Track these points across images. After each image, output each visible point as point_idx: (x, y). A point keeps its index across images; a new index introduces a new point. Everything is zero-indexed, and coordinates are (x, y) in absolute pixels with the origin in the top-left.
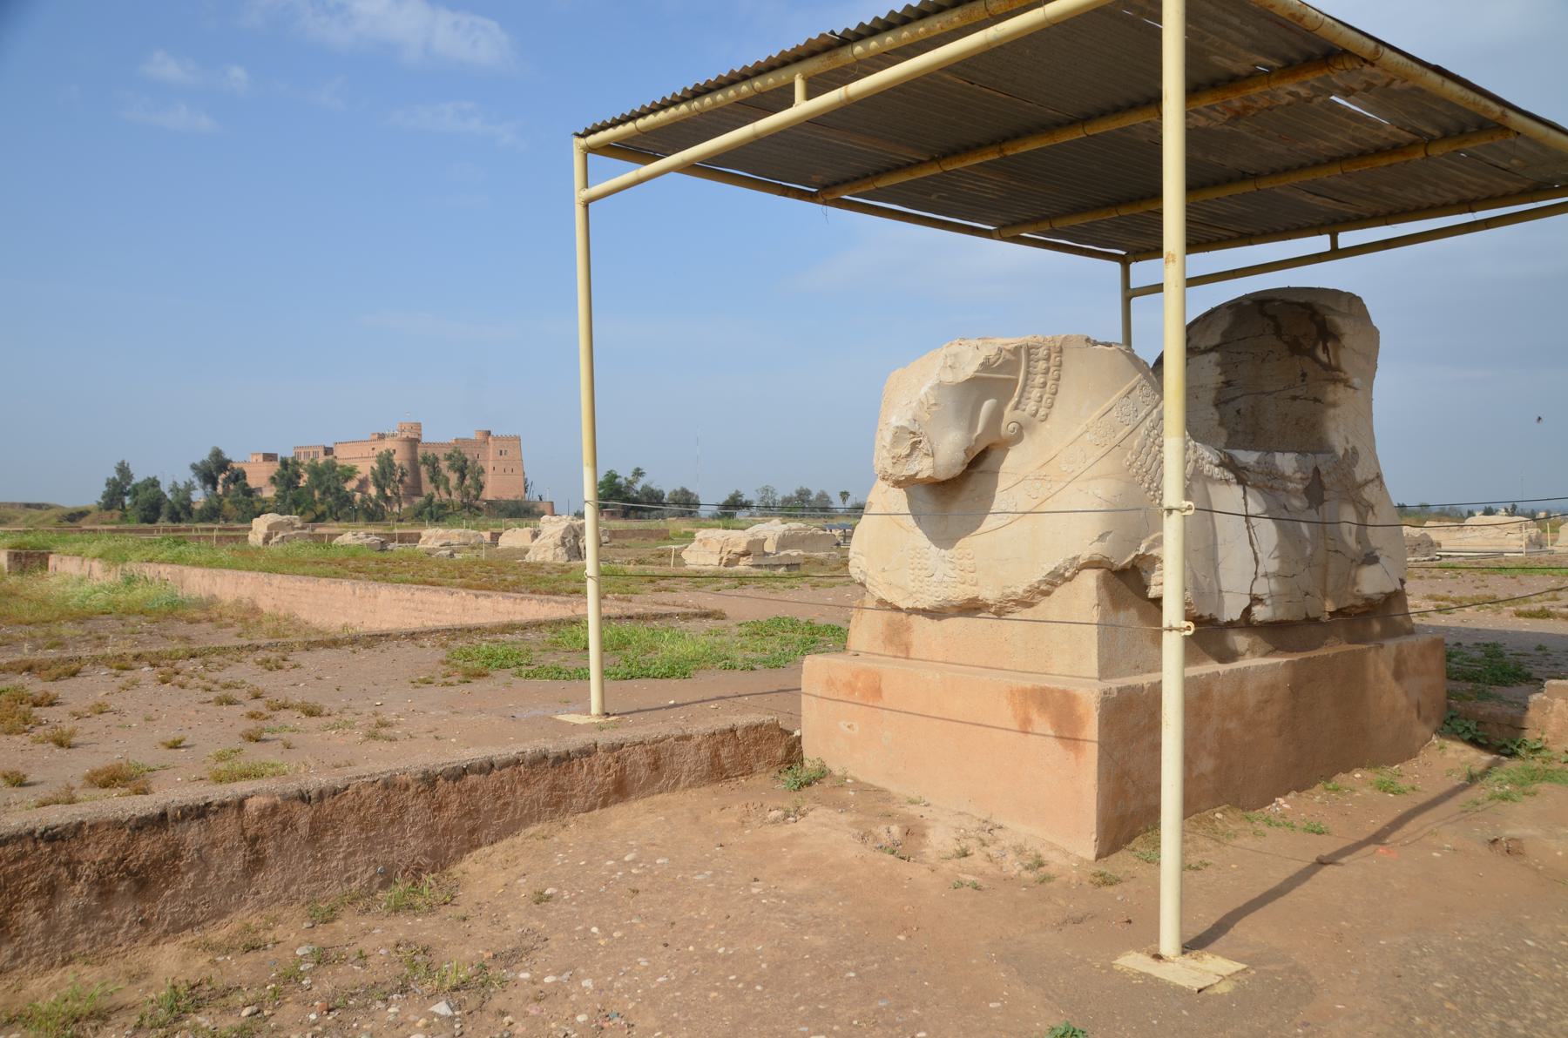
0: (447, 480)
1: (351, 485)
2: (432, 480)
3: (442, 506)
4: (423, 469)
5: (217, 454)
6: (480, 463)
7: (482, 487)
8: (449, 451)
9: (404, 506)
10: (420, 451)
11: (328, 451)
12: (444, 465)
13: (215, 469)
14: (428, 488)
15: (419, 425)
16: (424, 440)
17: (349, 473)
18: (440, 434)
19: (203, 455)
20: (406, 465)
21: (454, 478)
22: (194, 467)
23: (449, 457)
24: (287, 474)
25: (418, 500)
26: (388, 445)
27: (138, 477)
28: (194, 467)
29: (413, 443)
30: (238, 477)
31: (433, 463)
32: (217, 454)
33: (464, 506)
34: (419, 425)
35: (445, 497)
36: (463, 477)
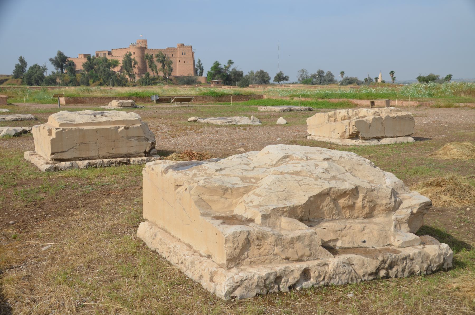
0: (156, 67)
1: (117, 69)
2: (150, 66)
3: (154, 79)
4: (147, 61)
5: (60, 54)
6: (172, 59)
7: (172, 70)
8: (157, 53)
9: (138, 78)
10: (146, 53)
11: (110, 53)
12: (155, 59)
13: (61, 61)
14: (149, 70)
15: (146, 41)
16: (148, 48)
17: (115, 64)
18: (155, 45)
19: (54, 55)
20: (138, 59)
21: (159, 66)
22: (51, 60)
23: (157, 56)
24: (91, 63)
25: (144, 76)
26: (132, 50)
27: (30, 64)
28: (51, 60)
29: (143, 49)
30: (72, 65)
31: (150, 58)
32: (60, 54)
33: (165, 79)
34: (146, 41)
35: (155, 74)
36: (164, 66)
